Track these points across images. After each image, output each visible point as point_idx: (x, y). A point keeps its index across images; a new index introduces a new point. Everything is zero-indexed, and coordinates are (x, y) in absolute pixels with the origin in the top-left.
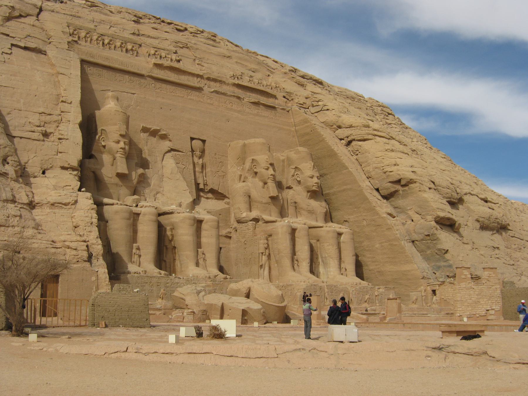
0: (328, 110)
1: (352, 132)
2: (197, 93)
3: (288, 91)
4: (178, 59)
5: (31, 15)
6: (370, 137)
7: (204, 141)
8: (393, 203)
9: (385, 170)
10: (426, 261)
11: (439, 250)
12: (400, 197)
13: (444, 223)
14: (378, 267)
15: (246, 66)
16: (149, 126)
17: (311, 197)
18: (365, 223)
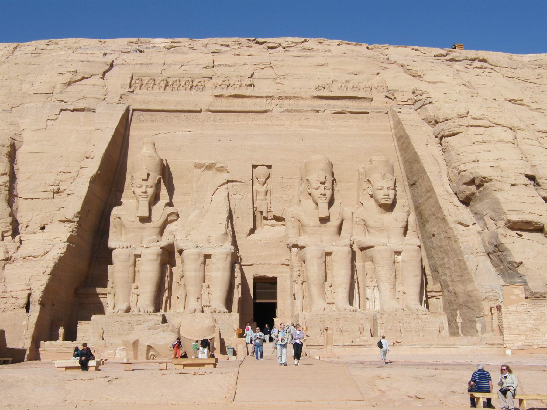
0: (430, 103)
3: (389, 88)
4: (249, 83)
5: (95, 75)
6: (460, 129)
7: (269, 167)
8: (473, 209)
9: (460, 169)
10: (502, 277)
11: (510, 263)
13: (523, 227)
16: (202, 162)
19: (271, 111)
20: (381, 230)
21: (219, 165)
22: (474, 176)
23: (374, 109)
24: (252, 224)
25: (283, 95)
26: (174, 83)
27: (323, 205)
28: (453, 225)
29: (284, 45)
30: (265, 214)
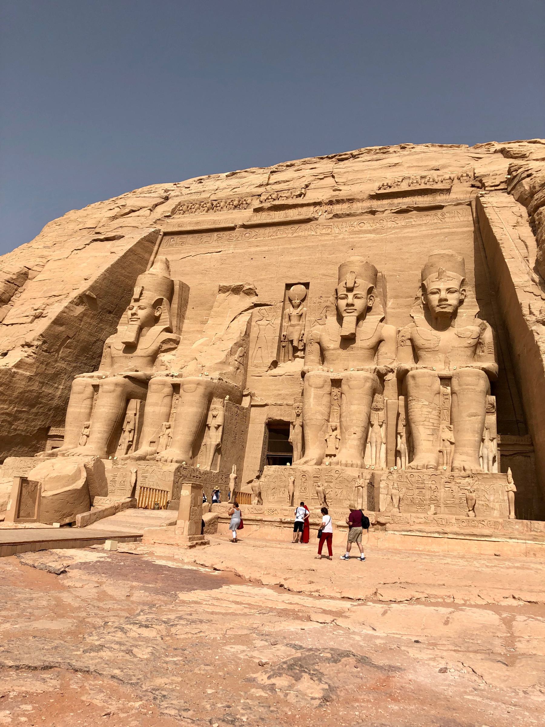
0: (529, 176)
2: (308, 225)
3: (476, 175)
5: (144, 207)
7: (307, 285)
19: (316, 219)
20: (434, 351)
21: (247, 287)
23: (453, 202)
24: (275, 355)
25: (334, 199)
26: (218, 205)
27: (350, 320)
28: (534, 328)
29: (355, 152)
30: (295, 344)
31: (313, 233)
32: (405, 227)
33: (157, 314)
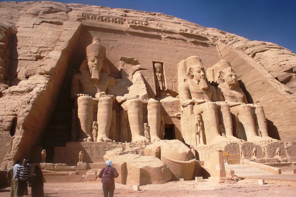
0: (239, 41)
1: (255, 48)
5: (63, 11)
6: (267, 49)
7: (162, 64)
8: (289, 85)
9: (280, 64)
12: (294, 81)
14: (284, 129)
15: (190, 27)
17: (232, 89)
18: (271, 100)
20: (233, 97)
22: (293, 66)
30: (161, 89)
31: (160, 42)
32: (196, 48)
33: (103, 67)
